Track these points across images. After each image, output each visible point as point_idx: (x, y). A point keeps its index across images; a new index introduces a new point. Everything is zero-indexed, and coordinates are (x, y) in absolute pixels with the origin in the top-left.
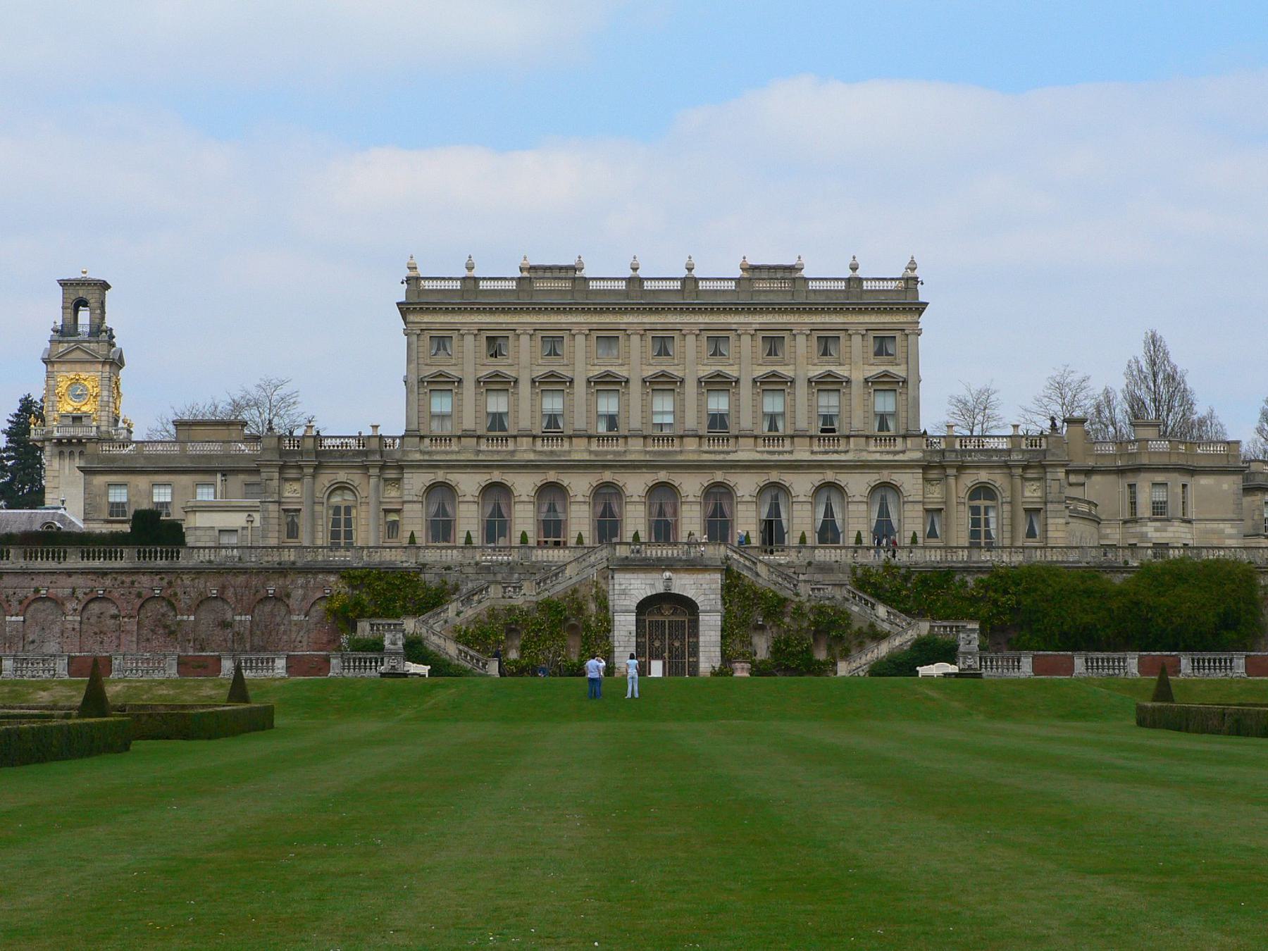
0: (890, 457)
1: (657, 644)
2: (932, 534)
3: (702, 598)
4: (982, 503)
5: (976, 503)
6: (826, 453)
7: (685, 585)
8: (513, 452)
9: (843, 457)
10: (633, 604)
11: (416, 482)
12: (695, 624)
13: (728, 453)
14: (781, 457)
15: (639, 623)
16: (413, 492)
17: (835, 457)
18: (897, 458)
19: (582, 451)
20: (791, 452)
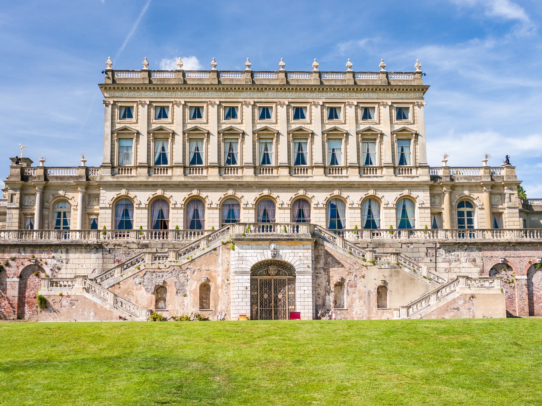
0: (409, 180)
1: (266, 296)
2: (376, 258)
3: (298, 263)
4: (465, 210)
5: (461, 209)
6: (370, 177)
7: (288, 255)
8: (170, 177)
9: (379, 180)
10: (248, 268)
11: (107, 197)
12: (292, 281)
13: (308, 177)
14: (341, 180)
15: (253, 282)
16: (106, 202)
17: (375, 179)
18: (414, 180)
19: (215, 176)
20: (347, 177)
